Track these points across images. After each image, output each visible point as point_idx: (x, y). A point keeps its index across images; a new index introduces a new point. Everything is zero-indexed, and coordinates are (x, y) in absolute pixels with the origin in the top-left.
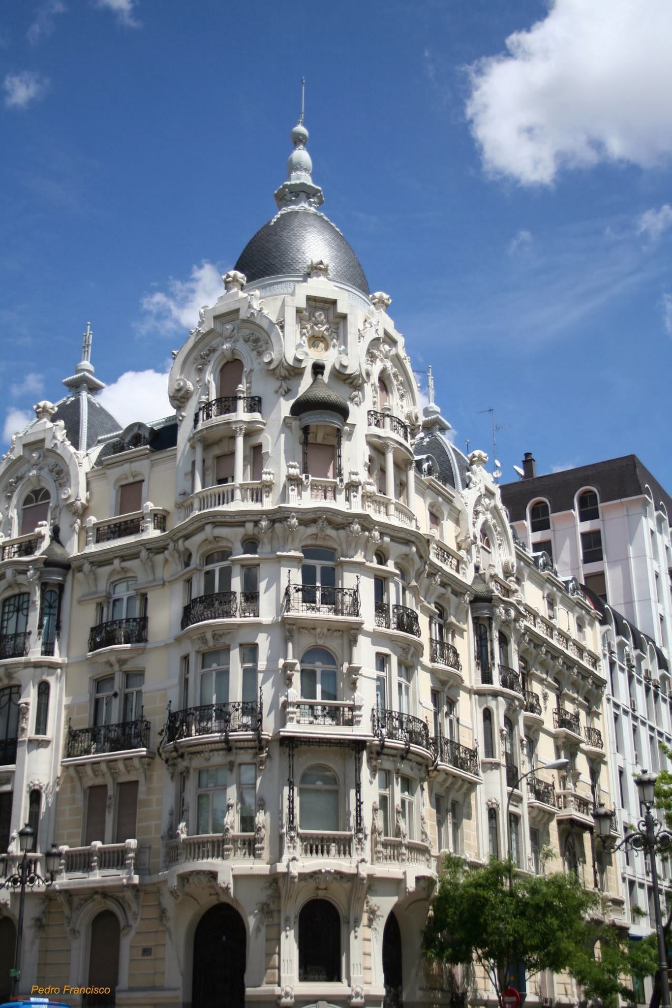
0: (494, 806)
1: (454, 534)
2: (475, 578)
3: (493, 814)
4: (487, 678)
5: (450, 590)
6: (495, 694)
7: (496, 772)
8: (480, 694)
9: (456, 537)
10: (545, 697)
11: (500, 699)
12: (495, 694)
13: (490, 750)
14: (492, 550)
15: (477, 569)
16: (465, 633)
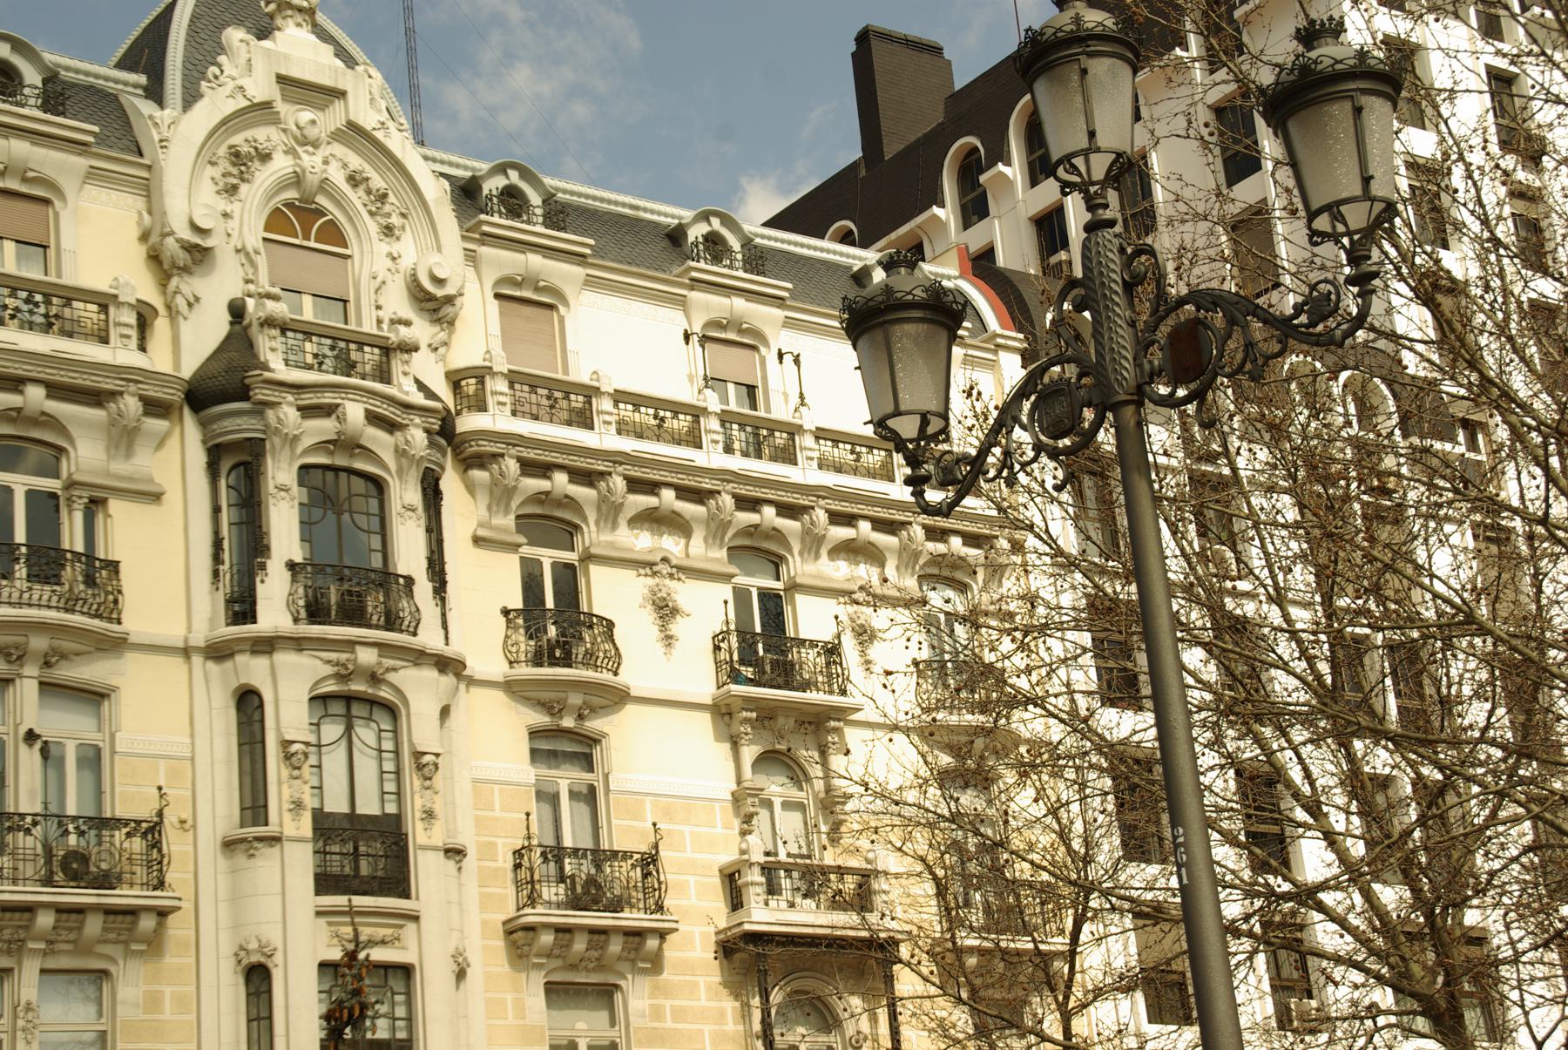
0: (254, 958)
1: (135, 233)
2: (228, 338)
3: (257, 977)
4: (243, 607)
5: (35, 393)
6: (266, 645)
7: (268, 860)
8: (219, 652)
9: (144, 237)
10: (665, 610)
11: (284, 658)
12: (266, 645)
13: (255, 806)
14: (353, 249)
15: (237, 311)
16: (173, 496)
